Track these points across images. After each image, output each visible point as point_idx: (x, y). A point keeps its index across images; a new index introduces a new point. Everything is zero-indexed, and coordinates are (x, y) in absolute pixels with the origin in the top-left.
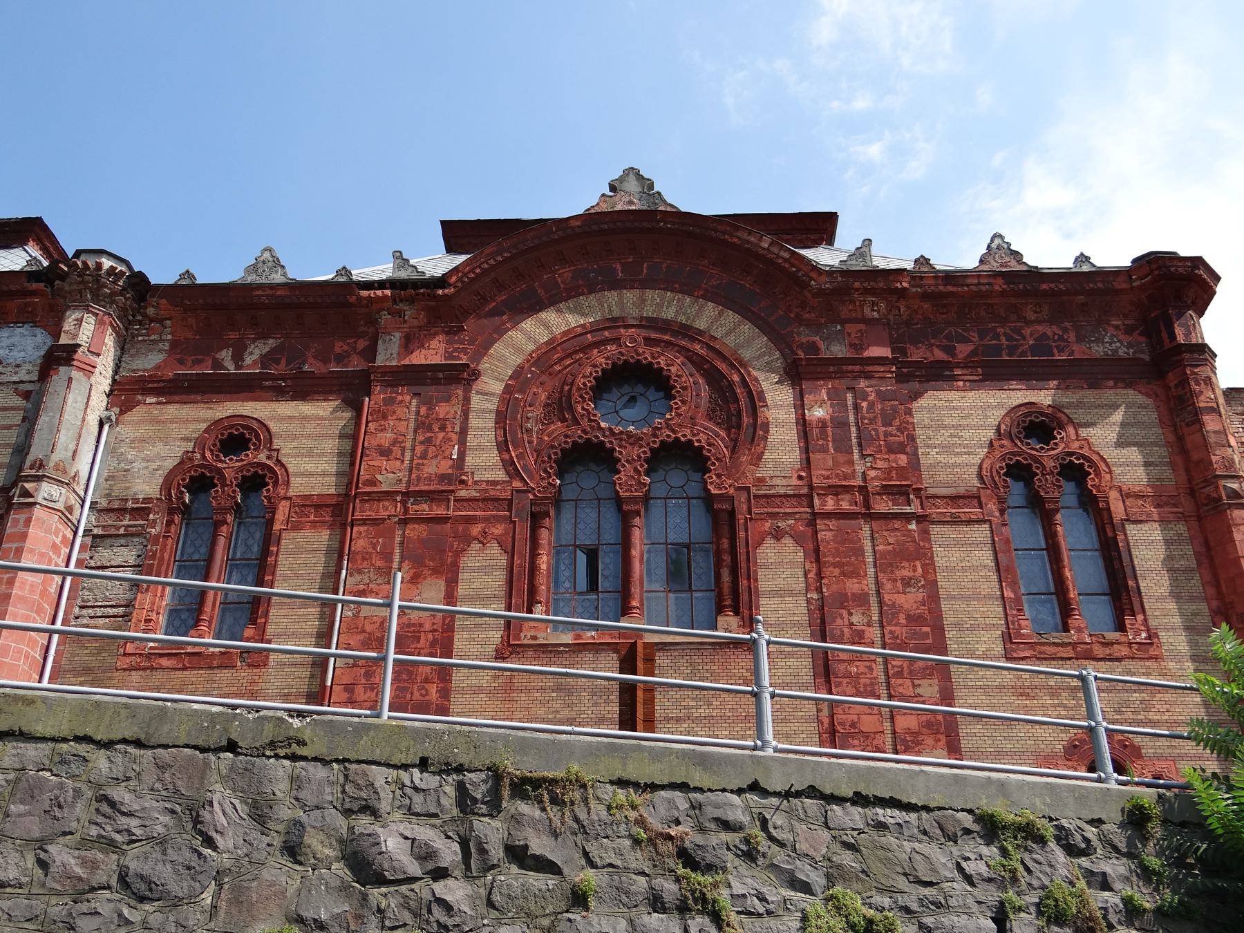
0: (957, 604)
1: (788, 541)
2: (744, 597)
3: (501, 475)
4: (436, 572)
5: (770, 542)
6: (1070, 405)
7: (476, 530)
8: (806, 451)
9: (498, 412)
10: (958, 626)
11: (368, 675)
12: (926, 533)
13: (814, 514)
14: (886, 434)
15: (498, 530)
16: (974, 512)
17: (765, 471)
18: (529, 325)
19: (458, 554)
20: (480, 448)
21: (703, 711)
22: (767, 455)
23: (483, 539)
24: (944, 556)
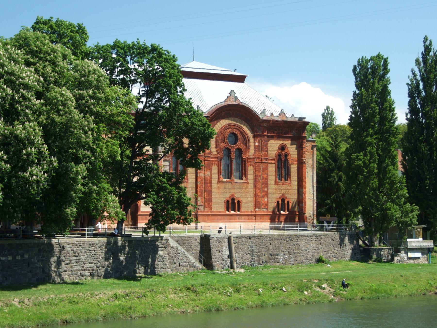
0: (270, 176)
1: (252, 166)
2: (246, 175)
3: (216, 153)
4: (209, 169)
5: (250, 166)
6: (287, 144)
7: (213, 163)
8: (255, 151)
9: (215, 141)
10: (270, 180)
11: (202, 185)
12: (268, 165)
13: (255, 162)
14: (265, 149)
15: (216, 163)
16: (273, 162)
17: (250, 154)
18: (218, 124)
19: (212, 166)
20: (213, 148)
21: (241, 192)
22: (250, 152)
23: (215, 164)
24: (270, 169)
